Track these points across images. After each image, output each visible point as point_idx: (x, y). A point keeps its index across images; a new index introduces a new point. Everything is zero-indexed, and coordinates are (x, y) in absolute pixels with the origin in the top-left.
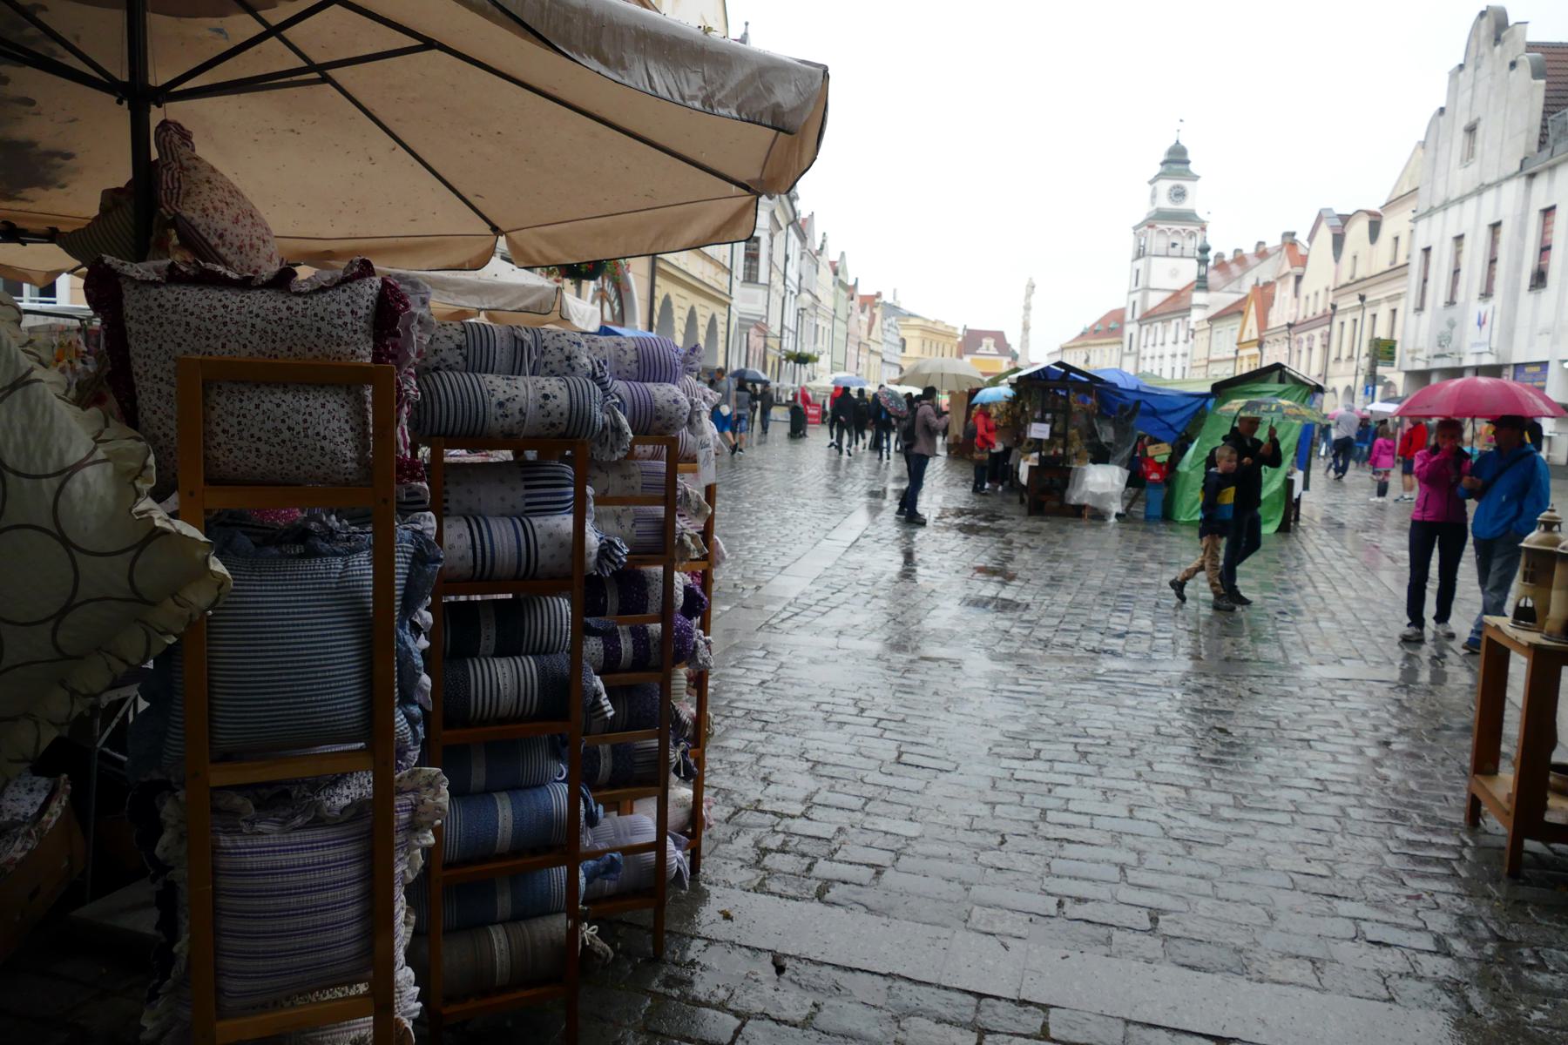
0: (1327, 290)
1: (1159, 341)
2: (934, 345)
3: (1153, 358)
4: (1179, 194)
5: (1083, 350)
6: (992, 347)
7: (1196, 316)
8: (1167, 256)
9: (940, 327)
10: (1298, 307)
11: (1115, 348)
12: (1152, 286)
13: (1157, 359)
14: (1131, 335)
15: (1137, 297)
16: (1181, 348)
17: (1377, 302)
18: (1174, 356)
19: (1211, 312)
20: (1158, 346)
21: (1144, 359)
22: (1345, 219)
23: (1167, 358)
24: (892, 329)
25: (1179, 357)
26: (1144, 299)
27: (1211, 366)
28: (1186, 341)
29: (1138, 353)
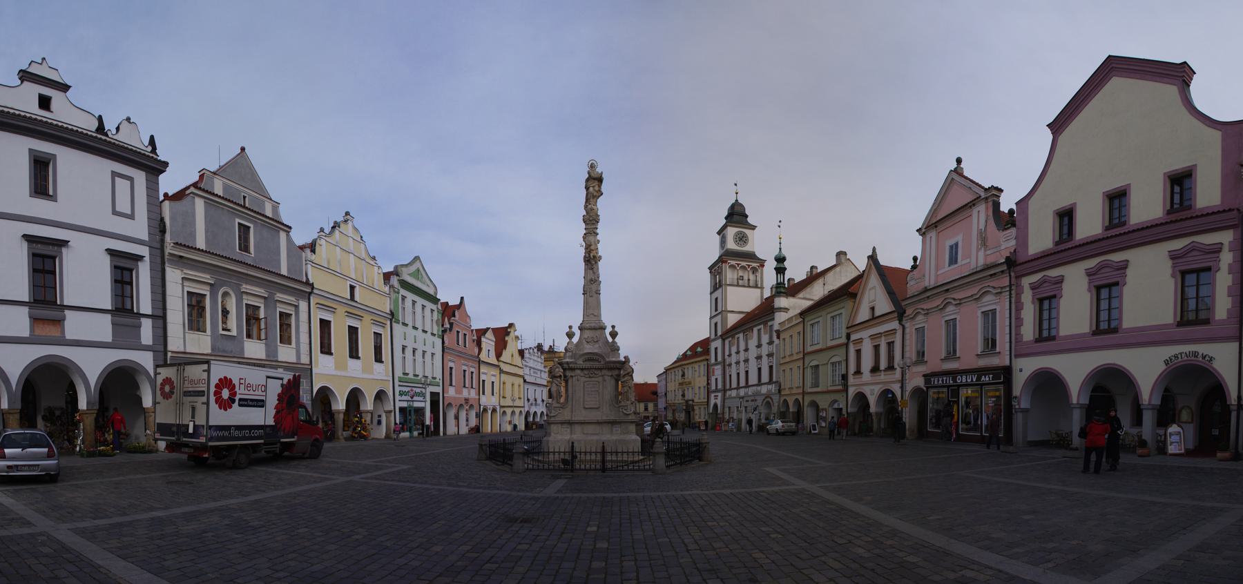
1: (742, 347)
3: (738, 363)
5: (680, 369)
7: (780, 317)
8: (738, 285)
13: (742, 364)
14: (716, 349)
15: (718, 319)
16: (765, 350)
18: (759, 358)
20: (742, 353)
21: (730, 365)
24: (536, 358)
25: (765, 359)
26: (724, 320)
27: (807, 359)
28: (771, 343)
29: (724, 360)
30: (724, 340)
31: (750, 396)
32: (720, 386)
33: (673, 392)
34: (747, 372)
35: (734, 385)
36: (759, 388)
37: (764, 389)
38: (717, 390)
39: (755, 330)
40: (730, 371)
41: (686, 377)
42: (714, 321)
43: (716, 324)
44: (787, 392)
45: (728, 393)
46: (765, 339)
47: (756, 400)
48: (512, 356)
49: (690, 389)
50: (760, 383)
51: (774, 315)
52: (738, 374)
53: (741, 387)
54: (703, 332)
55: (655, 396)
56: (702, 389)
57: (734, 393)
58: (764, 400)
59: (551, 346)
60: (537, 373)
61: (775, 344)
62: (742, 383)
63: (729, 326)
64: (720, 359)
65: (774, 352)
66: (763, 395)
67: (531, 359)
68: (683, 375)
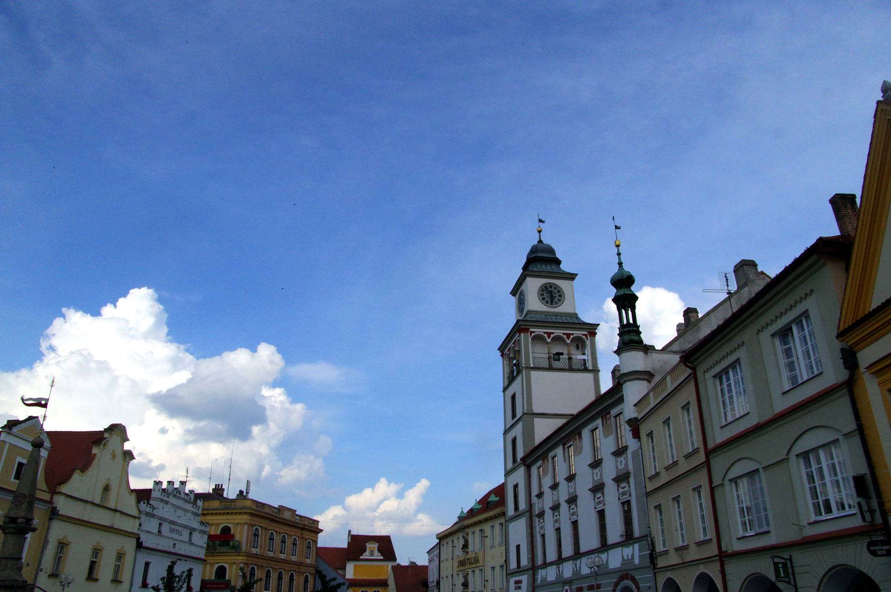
2: (277, 539)
3: (556, 508)
4: (551, 295)
5: (460, 535)
6: (376, 552)
9: (287, 515)
11: (497, 523)
12: (535, 411)
13: (564, 507)
14: (516, 487)
15: (518, 431)
16: (610, 469)
18: (598, 488)
20: (563, 486)
21: (541, 514)
26: (529, 432)
27: (719, 464)
30: (528, 468)
31: (587, 577)
32: (524, 562)
33: (450, 577)
34: (575, 524)
35: (552, 556)
36: (604, 556)
37: (615, 559)
38: (519, 570)
39: (586, 433)
40: (542, 528)
41: (471, 548)
42: (510, 436)
43: (514, 441)
44: (673, 559)
45: (541, 573)
47: (599, 586)
48: (107, 489)
49: (477, 571)
50: (605, 546)
51: (621, 391)
52: (558, 530)
53: (568, 559)
55: (425, 588)
56: (498, 569)
57: (550, 574)
58: (617, 584)
59: (241, 492)
60: (179, 533)
61: (629, 451)
64: (522, 506)
65: (631, 468)
66: (615, 571)
67: (167, 502)
68: (465, 546)
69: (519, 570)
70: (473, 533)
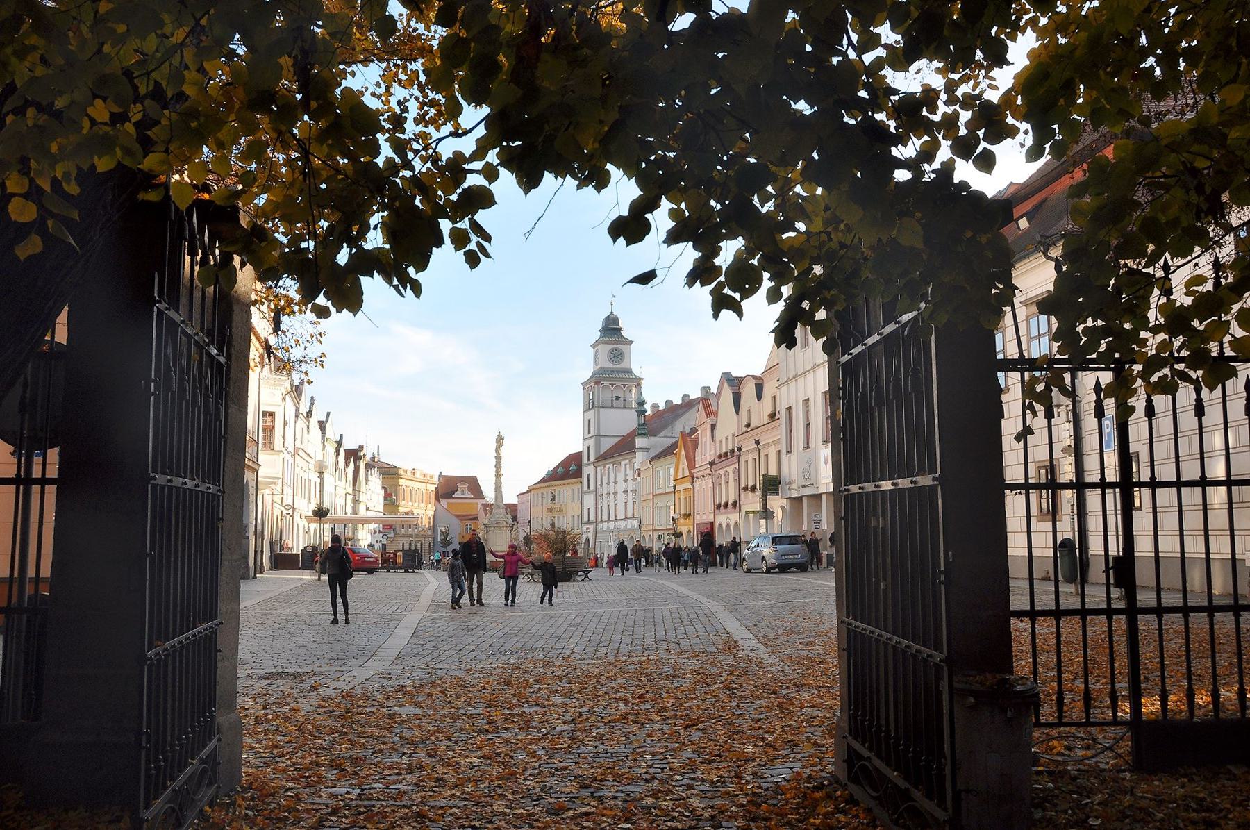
0: (733, 435)
1: (612, 480)
3: (608, 494)
4: (617, 355)
5: (549, 490)
6: (466, 492)
10: (715, 449)
13: (612, 495)
14: (589, 475)
17: (768, 445)
19: (653, 454)
20: (612, 484)
22: (741, 380)
23: (620, 494)
25: (630, 493)
28: (634, 480)
32: (592, 518)
35: (605, 518)
38: (589, 522)
45: (600, 526)
46: (630, 476)
49: (561, 518)
50: (626, 518)
54: (577, 447)
56: (576, 518)
62: (612, 518)
63: (602, 453)
68: (553, 500)
69: (589, 522)
70: (559, 491)
